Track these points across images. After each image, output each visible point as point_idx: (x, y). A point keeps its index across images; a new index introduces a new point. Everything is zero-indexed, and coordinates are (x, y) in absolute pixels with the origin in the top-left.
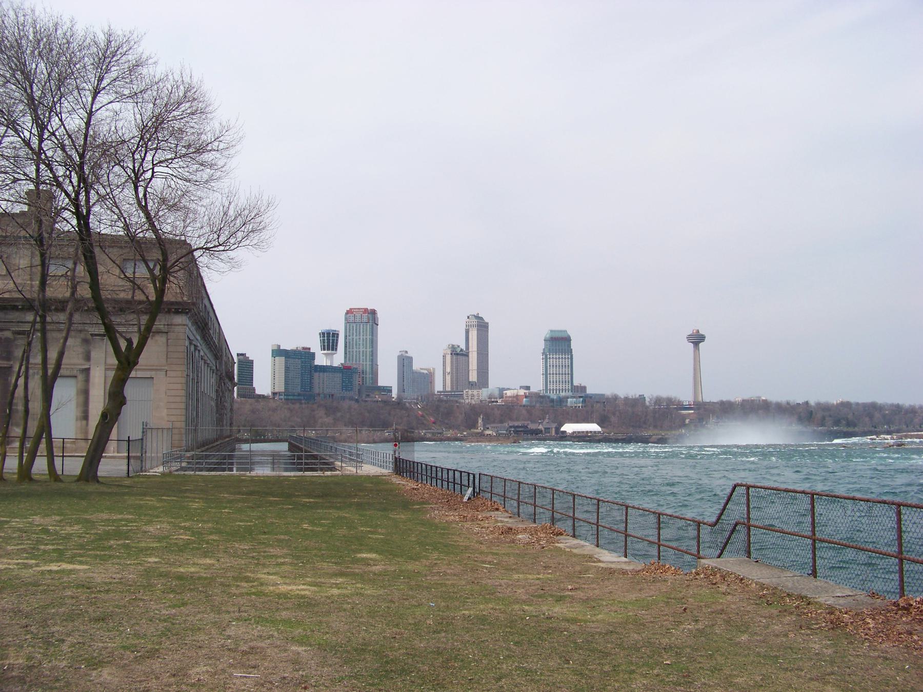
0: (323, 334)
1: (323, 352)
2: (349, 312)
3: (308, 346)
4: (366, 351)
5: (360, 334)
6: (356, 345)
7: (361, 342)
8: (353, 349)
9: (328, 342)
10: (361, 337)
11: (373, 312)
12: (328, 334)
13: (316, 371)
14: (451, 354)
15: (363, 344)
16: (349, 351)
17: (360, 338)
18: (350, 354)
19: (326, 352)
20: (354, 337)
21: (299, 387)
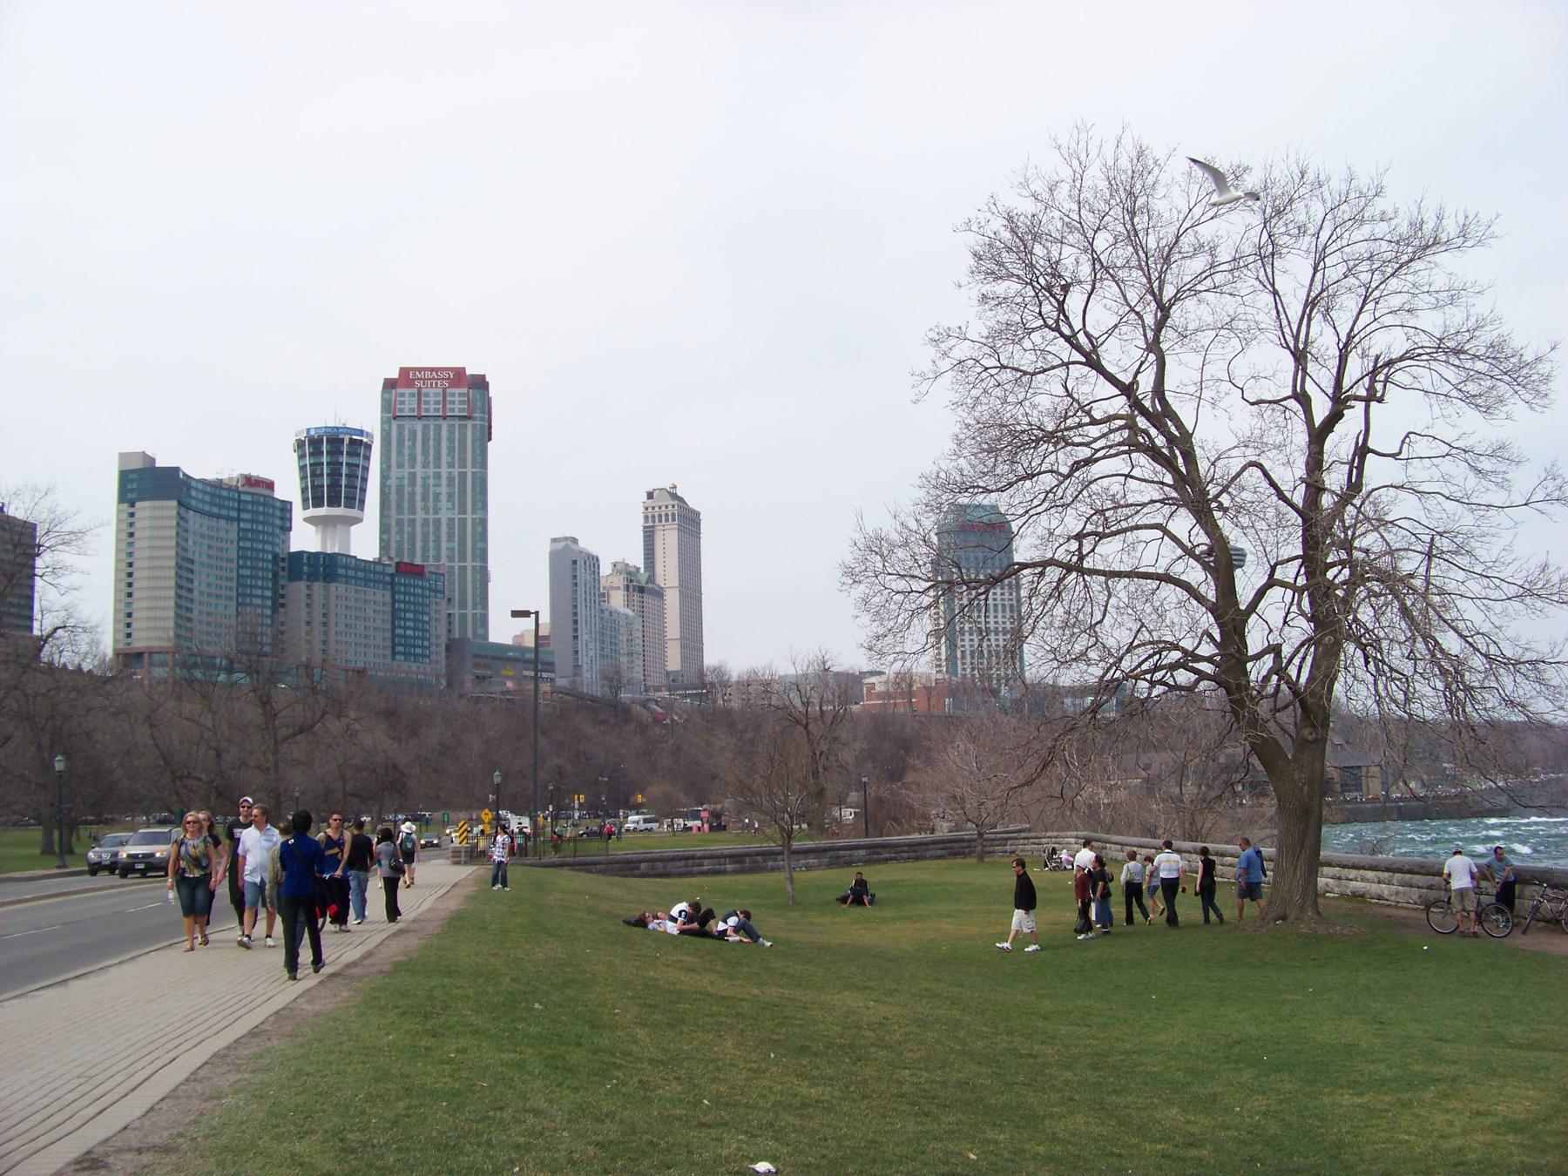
0: (315, 442)
1: (313, 512)
4: (463, 522)
5: (438, 459)
6: (425, 498)
7: (444, 490)
8: (413, 511)
9: (335, 474)
10: (444, 470)
11: (480, 383)
13: (294, 575)
15: (450, 496)
16: (400, 523)
17: (438, 476)
18: (401, 532)
20: (419, 470)
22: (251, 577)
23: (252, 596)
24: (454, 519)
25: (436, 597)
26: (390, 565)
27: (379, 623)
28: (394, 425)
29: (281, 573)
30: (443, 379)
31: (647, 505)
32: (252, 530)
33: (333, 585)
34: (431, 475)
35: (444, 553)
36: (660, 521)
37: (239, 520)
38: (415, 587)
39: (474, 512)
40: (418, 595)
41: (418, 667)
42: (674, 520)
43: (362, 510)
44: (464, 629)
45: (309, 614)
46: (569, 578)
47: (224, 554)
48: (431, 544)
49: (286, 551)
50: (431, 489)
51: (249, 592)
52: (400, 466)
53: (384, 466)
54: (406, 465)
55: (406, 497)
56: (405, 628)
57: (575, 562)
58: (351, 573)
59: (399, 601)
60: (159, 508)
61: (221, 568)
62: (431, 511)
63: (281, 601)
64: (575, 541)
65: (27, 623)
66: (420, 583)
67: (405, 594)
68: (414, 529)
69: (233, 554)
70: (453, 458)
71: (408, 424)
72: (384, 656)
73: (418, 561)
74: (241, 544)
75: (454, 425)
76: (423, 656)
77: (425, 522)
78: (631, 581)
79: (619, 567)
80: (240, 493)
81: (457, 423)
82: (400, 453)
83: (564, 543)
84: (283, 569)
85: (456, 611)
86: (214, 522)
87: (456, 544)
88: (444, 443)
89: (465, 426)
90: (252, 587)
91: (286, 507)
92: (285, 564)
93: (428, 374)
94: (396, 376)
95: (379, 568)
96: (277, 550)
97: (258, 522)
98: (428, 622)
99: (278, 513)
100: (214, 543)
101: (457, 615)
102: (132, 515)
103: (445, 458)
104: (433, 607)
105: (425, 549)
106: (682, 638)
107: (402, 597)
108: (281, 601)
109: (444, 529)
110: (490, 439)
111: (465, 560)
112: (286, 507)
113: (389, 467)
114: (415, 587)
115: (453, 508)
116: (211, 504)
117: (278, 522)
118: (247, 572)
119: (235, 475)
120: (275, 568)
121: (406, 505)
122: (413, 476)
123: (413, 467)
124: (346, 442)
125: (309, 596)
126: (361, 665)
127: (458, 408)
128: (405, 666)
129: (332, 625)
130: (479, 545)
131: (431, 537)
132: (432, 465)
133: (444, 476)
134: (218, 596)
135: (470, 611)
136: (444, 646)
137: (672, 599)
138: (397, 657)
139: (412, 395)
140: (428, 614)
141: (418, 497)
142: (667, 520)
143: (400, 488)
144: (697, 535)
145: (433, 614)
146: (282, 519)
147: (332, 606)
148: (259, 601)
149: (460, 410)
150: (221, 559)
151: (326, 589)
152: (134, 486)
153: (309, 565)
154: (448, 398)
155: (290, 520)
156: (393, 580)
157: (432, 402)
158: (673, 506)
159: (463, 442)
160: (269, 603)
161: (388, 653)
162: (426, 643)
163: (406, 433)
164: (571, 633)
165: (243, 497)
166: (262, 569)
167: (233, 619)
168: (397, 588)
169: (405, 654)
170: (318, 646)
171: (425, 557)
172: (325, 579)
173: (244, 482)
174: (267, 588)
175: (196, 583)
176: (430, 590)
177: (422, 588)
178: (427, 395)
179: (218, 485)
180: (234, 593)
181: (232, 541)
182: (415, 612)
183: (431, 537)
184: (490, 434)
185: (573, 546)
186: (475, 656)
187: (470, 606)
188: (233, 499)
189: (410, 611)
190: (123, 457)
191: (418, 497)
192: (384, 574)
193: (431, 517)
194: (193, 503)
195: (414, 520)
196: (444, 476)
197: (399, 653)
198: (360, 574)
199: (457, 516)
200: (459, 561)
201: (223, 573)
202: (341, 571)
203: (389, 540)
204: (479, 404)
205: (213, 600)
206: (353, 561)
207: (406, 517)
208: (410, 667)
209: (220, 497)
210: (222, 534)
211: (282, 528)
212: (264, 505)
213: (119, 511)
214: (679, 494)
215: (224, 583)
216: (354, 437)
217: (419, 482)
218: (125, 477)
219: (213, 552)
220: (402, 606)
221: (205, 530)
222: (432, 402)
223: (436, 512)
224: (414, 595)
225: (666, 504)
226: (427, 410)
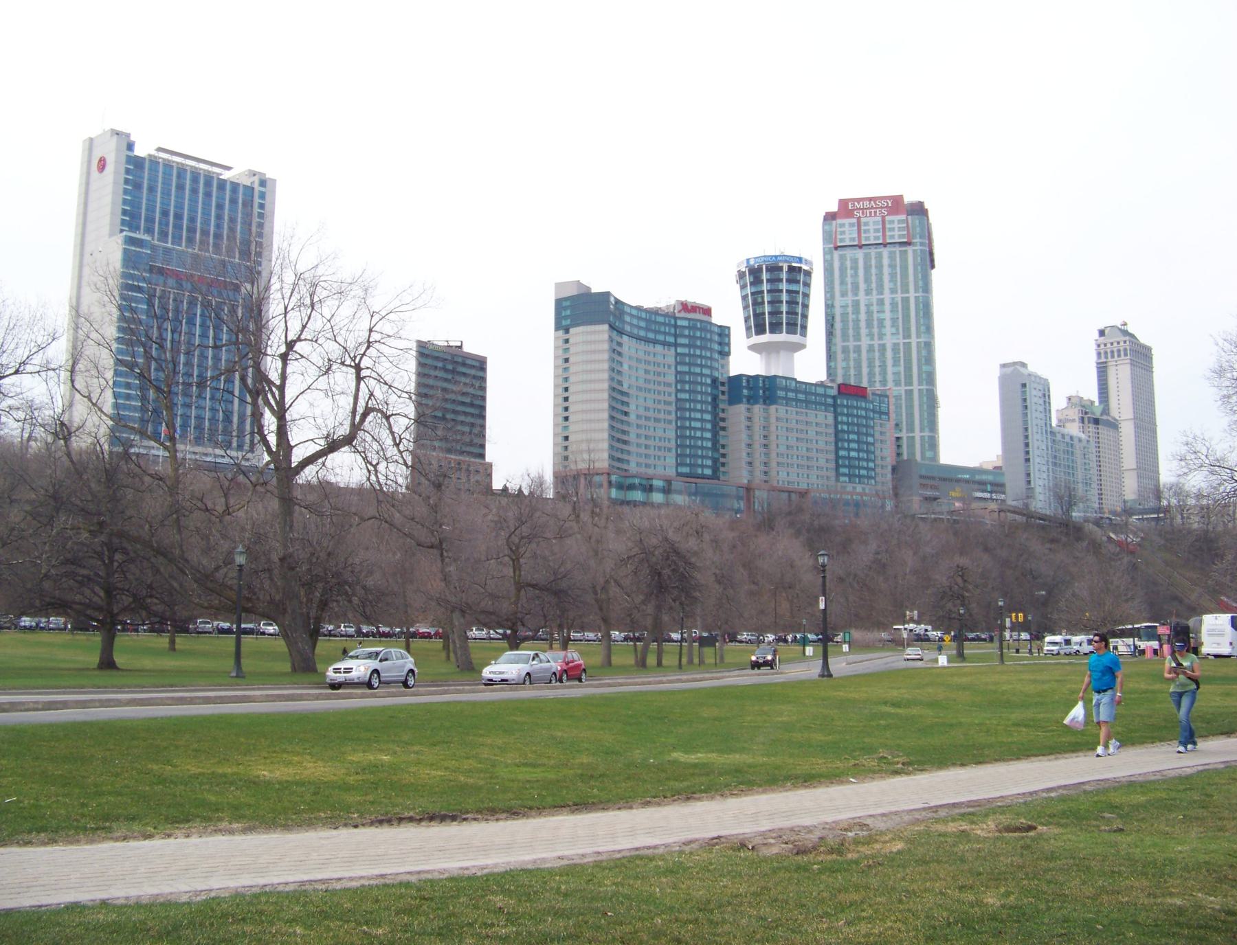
0: (755, 272)
2: (846, 208)
4: (908, 346)
6: (869, 324)
7: (887, 315)
8: (857, 337)
10: (887, 296)
12: (774, 268)
13: (734, 399)
14: (1082, 420)
15: (894, 321)
16: (845, 350)
17: (881, 302)
18: (846, 359)
19: (767, 337)
21: (671, 460)
22: (690, 401)
23: (690, 419)
24: (898, 344)
25: (880, 419)
26: (832, 388)
27: (821, 445)
28: (836, 254)
29: (721, 397)
31: (1099, 342)
32: (689, 355)
33: (773, 408)
34: (875, 301)
35: (890, 377)
36: (1113, 356)
37: (676, 345)
38: (857, 408)
39: (918, 336)
40: (861, 417)
41: (864, 489)
42: (1126, 355)
43: (805, 336)
44: (911, 453)
45: (750, 437)
46: (1019, 401)
47: (661, 379)
48: (877, 370)
49: (725, 376)
50: (875, 316)
51: (688, 415)
52: (844, 294)
53: (828, 295)
54: (850, 293)
55: (851, 324)
56: (849, 450)
57: (1024, 385)
58: (791, 395)
59: (843, 423)
60: (588, 333)
61: (659, 393)
62: (876, 337)
63: (722, 424)
64: (1024, 365)
65: (479, 451)
66: (863, 405)
67: (848, 415)
68: (859, 355)
69: (671, 378)
70: (895, 284)
71: (849, 253)
72: (828, 478)
73: (865, 384)
74: (679, 368)
75: (895, 252)
76: (869, 477)
77: (871, 349)
78: (1086, 413)
79: (1073, 400)
80: (676, 318)
81: (898, 249)
82: (843, 282)
83: (1012, 368)
84: (723, 393)
85: (904, 434)
86: (650, 348)
87: (902, 369)
88: (886, 270)
89: (906, 252)
90: (690, 410)
91: (724, 332)
92: (725, 388)
93: (867, 204)
94: (834, 208)
95: (820, 390)
96: (716, 374)
97: (696, 347)
98: (873, 444)
99: (716, 338)
100: (651, 368)
101: (905, 439)
102: (567, 341)
103: (887, 285)
104: (877, 428)
105: (871, 374)
106: (1138, 468)
107: (845, 419)
108: (722, 424)
109: (889, 354)
110: (933, 267)
111: (911, 384)
112: (724, 332)
113: (833, 297)
114: (857, 408)
115: (898, 333)
116: (647, 329)
117: (716, 347)
118: (686, 396)
119: (672, 302)
120: (715, 392)
121: (851, 332)
122: (856, 304)
123: (856, 294)
124: (785, 269)
125: (749, 419)
126: (803, 486)
127: (896, 235)
128: (849, 488)
129: (773, 446)
130: (925, 368)
131: (877, 363)
132: (874, 292)
133: (887, 302)
134: (657, 420)
135: (917, 434)
136: (890, 468)
137: (1127, 431)
138: (842, 479)
139: (851, 225)
140: (873, 436)
141: (863, 324)
142: (1119, 356)
143: (844, 316)
144: (1149, 369)
145: (877, 435)
146: (720, 344)
147: (773, 428)
148: (698, 425)
149: (900, 236)
150: (659, 383)
151: (766, 411)
152: (568, 312)
153: (748, 388)
154: (888, 226)
155: (729, 344)
156: (835, 401)
157: (872, 231)
158: (1125, 342)
159: (904, 268)
160: (709, 426)
161: (833, 474)
162: (871, 465)
163: (848, 264)
164: (1022, 456)
165: (679, 323)
166: (701, 393)
167: (673, 442)
168: (839, 410)
169: (849, 476)
170: (759, 467)
171: (871, 382)
172: (764, 401)
173: (680, 308)
174: (706, 412)
175: (632, 407)
176: (874, 411)
177: (866, 409)
178: (866, 224)
179: (655, 312)
180: (673, 417)
181: (669, 367)
182: (858, 433)
183: (877, 363)
184: (932, 261)
185: (1022, 370)
186: (922, 477)
188: (669, 325)
189: (854, 433)
190: (559, 286)
191: (863, 324)
192: (825, 396)
193: (876, 343)
194: (628, 328)
195: (859, 347)
196: (887, 302)
197: (845, 475)
198: (801, 396)
199: (901, 341)
200: (906, 385)
201: (661, 397)
202: (781, 393)
203: (835, 368)
204: (918, 230)
205: (651, 424)
206: (793, 384)
207: (851, 344)
208: (854, 488)
209: (656, 322)
210: (660, 359)
211: (721, 353)
212: (701, 330)
213: (556, 338)
214: (1130, 331)
215: (661, 407)
216: (794, 264)
217: (863, 309)
218: (560, 304)
219: (650, 377)
220: (845, 428)
221: (641, 354)
222: (872, 231)
223: (880, 338)
224: (858, 416)
225: (1118, 339)
226: (867, 238)
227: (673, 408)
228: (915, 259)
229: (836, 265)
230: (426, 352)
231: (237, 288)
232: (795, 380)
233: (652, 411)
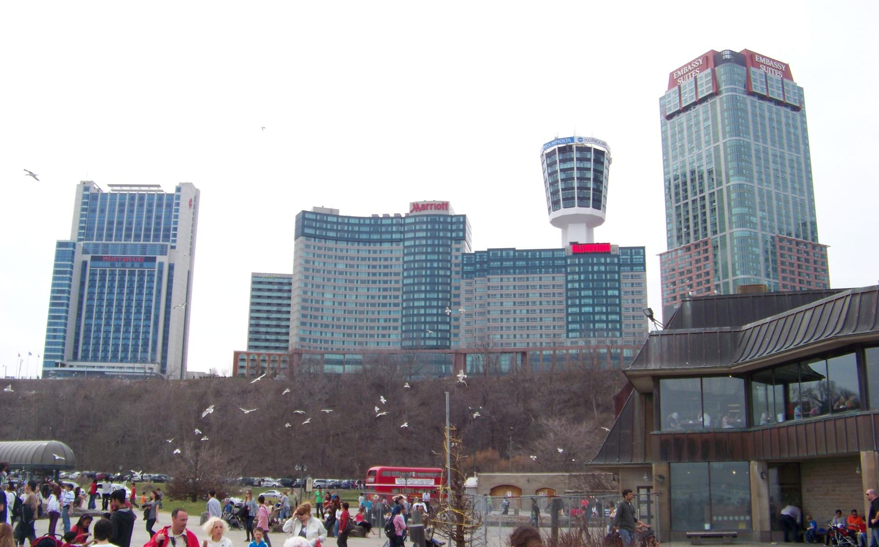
3: (439, 198)
21: (395, 336)
25: (632, 270)
30: (695, 68)
66: (603, 260)
103: (703, 139)
123: (683, 156)
126: (520, 346)
149: (707, 89)
159: (714, 117)
169: (580, 331)
187: (730, 274)
227: (400, 293)
228: (721, 106)
229: (669, 134)
230: (260, 280)
231: (153, 260)
232: (514, 249)
233: (377, 298)
